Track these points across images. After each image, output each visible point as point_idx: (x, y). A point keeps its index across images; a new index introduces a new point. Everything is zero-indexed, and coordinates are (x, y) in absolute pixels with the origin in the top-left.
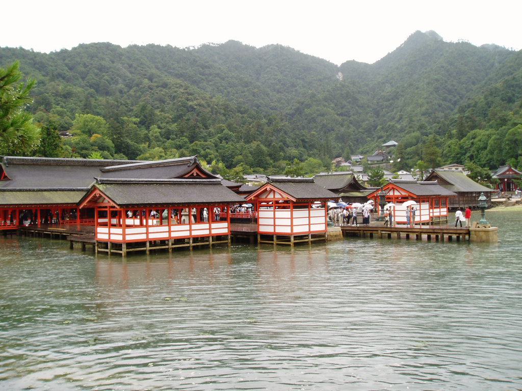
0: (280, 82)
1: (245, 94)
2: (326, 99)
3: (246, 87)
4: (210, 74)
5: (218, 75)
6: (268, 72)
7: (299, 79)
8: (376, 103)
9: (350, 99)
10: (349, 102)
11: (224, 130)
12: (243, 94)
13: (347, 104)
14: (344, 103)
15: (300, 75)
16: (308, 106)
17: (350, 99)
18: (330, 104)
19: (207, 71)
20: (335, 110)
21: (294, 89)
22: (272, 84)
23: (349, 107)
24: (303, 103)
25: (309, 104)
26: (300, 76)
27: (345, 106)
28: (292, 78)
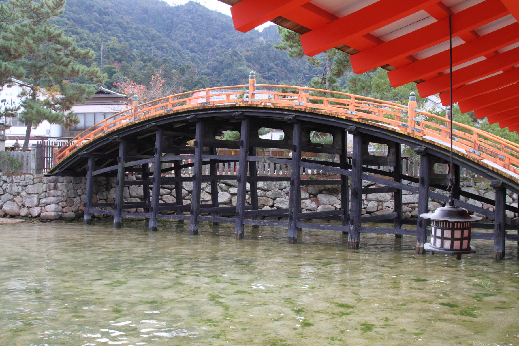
0: (194, 40)
1: (151, 48)
2: (248, 59)
3: (153, 40)
4: (109, 23)
5: (119, 24)
6: (180, 28)
7: (217, 38)
8: (308, 68)
9: (278, 61)
10: (277, 65)
11: (115, 72)
12: (149, 48)
13: (275, 67)
14: (272, 64)
15: (217, 34)
16: (230, 66)
17: (278, 61)
18: (255, 66)
19: (106, 18)
20: (260, 73)
21: (210, 50)
22: (185, 41)
23: (277, 70)
24: (222, 62)
25: (230, 64)
26: (218, 36)
27: (272, 68)
28: (208, 37)
